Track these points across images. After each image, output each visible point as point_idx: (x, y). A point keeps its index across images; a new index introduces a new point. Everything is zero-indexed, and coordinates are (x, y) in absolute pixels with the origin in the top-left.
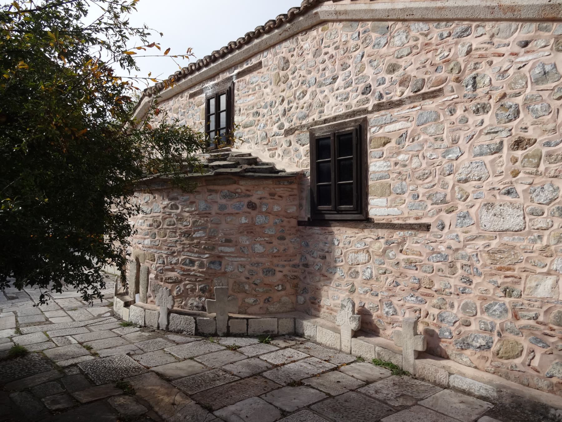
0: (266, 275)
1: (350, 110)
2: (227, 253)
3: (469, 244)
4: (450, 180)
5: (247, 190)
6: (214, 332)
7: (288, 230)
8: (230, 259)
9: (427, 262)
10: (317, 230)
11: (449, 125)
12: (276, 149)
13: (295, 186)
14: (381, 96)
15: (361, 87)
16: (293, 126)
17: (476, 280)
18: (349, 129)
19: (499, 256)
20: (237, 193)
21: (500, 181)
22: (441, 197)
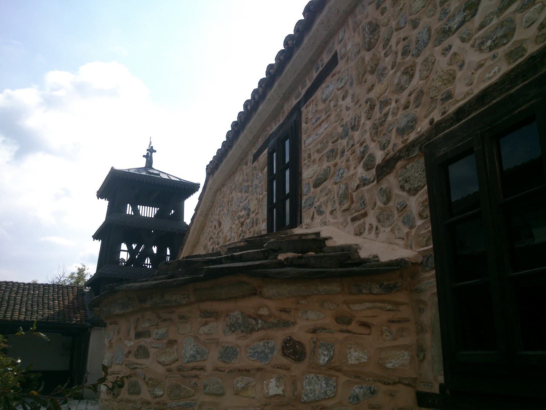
5: (283, 310)
12: (365, 215)
13: (401, 297)
16: (392, 153)
18: (523, 108)
20: (260, 316)
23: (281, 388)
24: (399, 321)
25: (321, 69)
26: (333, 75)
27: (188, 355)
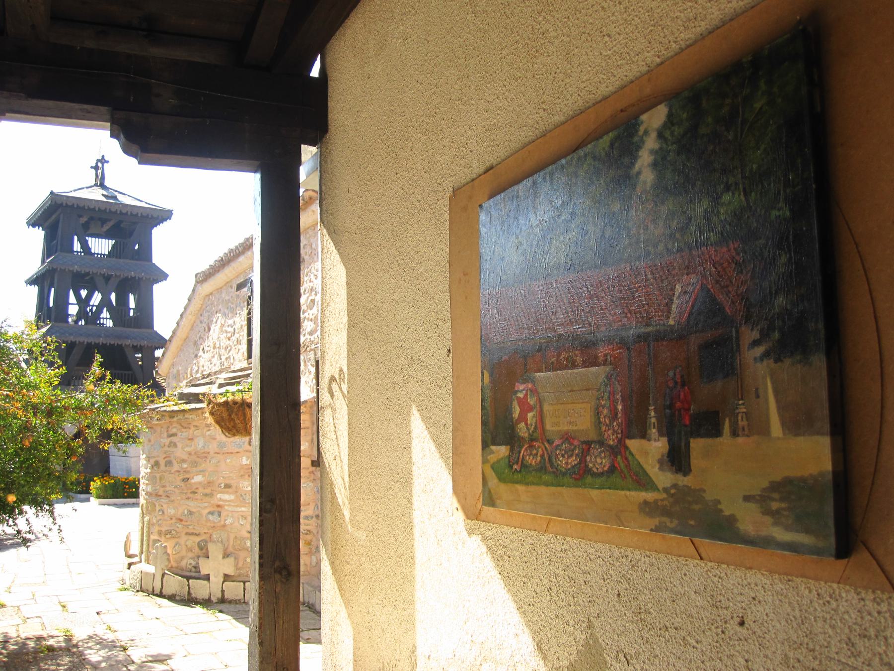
2: (226, 501)
6: (207, 598)
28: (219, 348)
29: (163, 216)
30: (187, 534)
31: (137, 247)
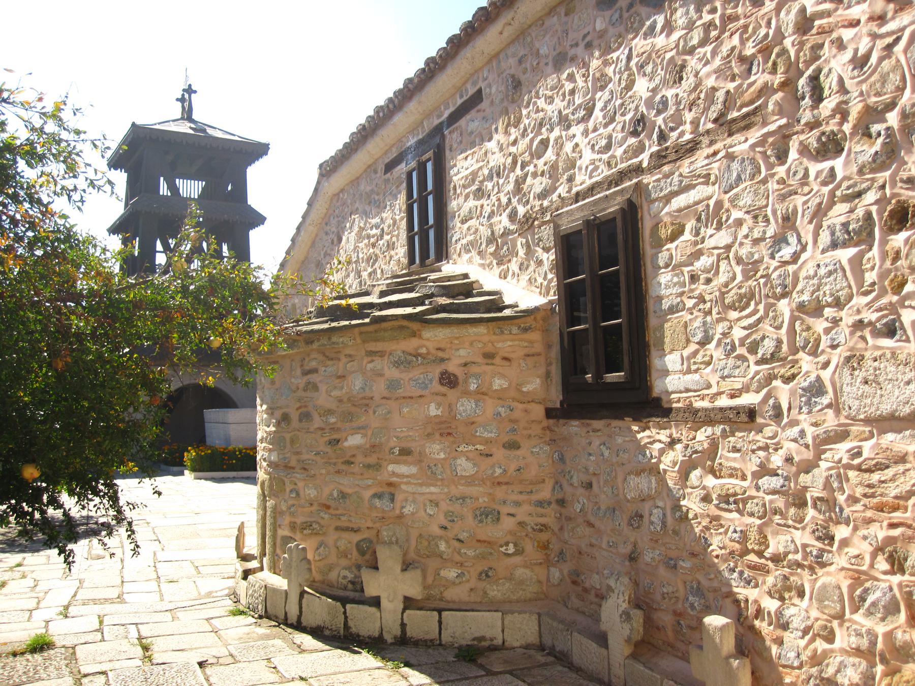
0: (481, 521)
1: (614, 170)
2: (403, 476)
3: (825, 451)
4: (784, 307)
6: (376, 634)
7: (525, 429)
8: (410, 489)
9: (753, 493)
10: (574, 427)
11: (776, 186)
14: (663, 137)
15: (631, 120)
17: (841, 532)
19: (875, 477)
20: (420, 355)
21: (869, 305)
22: (768, 346)
23: (441, 409)
24: (533, 355)
25: (465, 98)
26: (478, 111)
27: (357, 388)
28: (357, 262)
29: (258, 151)
30: (337, 528)
31: (229, 188)
